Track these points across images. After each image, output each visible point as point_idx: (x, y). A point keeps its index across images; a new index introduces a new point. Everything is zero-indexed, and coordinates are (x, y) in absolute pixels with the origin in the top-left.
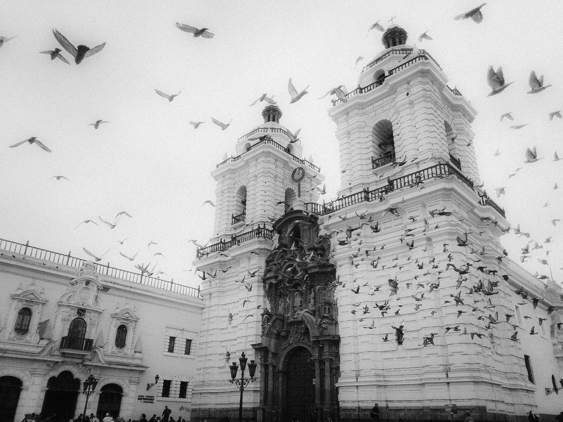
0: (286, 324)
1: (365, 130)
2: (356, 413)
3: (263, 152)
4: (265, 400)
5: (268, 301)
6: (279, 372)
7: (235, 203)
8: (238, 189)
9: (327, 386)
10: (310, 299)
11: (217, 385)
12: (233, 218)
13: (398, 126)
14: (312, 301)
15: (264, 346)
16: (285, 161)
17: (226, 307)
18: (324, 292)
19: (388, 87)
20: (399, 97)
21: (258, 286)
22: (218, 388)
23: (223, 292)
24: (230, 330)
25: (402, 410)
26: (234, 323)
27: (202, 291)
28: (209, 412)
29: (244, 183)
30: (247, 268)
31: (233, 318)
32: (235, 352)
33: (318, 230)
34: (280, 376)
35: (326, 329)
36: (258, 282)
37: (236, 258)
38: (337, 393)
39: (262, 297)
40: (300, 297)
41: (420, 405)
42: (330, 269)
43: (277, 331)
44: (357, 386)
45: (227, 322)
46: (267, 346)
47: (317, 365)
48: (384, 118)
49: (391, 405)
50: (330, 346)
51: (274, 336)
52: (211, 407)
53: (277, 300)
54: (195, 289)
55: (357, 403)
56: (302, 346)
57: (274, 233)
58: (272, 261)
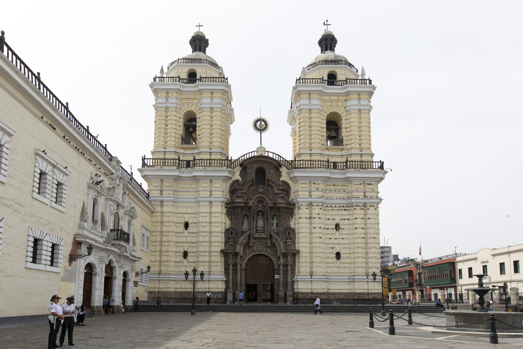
0: (252, 237)
1: (322, 112)
2: (311, 295)
3: (222, 90)
5: (227, 218)
7: (182, 124)
8: (185, 112)
9: (289, 280)
10: (272, 224)
11: (173, 275)
12: (182, 138)
13: (346, 122)
14: (275, 225)
17: (180, 215)
18: (284, 220)
19: (346, 91)
20: (352, 101)
21: (222, 206)
23: (176, 202)
25: (337, 294)
26: (191, 229)
27: (152, 197)
29: (193, 108)
30: (208, 189)
31: (189, 225)
32: (194, 252)
33: (280, 175)
35: (290, 245)
36: (222, 202)
37: (197, 177)
41: (348, 291)
42: (291, 207)
43: (246, 243)
45: (184, 229)
47: (281, 267)
48: (337, 111)
49: (330, 291)
51: (243, 245)
53: (241, 219)
55: (311, 290)
56: (264, 254)
57: (233, 166)
58: (242, 189)
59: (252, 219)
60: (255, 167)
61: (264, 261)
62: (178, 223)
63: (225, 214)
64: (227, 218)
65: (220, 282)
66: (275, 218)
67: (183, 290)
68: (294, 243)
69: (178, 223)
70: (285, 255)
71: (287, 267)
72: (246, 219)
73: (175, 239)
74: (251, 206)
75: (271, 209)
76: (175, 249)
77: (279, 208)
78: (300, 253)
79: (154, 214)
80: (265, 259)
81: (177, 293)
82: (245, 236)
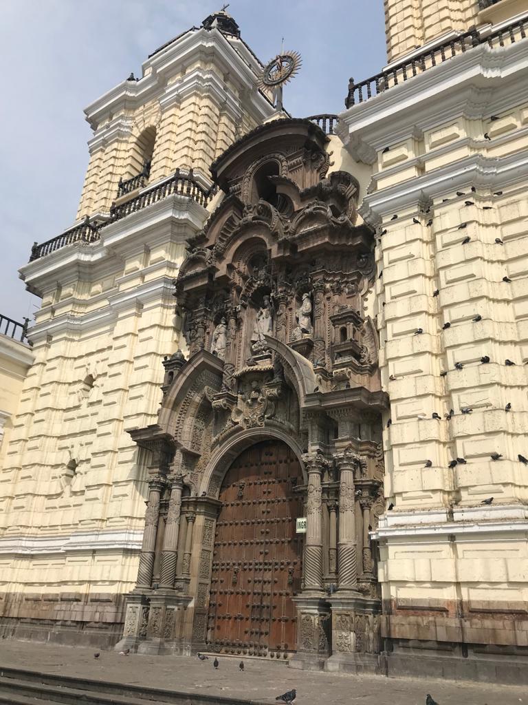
4: (150, 577)
5: (183, 341)
6: (197, 503)
11: (34, 538)
12: (121, 185)
15: (163, 432)
16: (242, 85)
22: (36, 544)
24: (85, 410)
28: (7, 601)
34: (200, 513)
38: (376, 556)
39: (171, 332)
40: (270, 318)
43: (204, 398)
44: (452, 537)
46: (172, 433)
50: (357, 427)
51: (192, 410)
52: (13, 591)
54: (16, 324)
55: (453, 589)
56: (268, 433)
59: (232, 321)
60: (251, 170)
61: (283, 465)
62: (75, 383)
63: (176, 329)
64: (185, 339)
65: (120, 558)
66: (304, 297)
67: (43, 590)
68: (374, 369)
69: (75, 383)
70: (327, 423)
71: (337, 477)
72: (221, 327)
73: (57, 431)
74: (225, 278)
75: (288, 271)
76: (53, 458)
77: (312, 258)
78: (393, 406)
79: (31, 371)
80: (284, 458)
81: (27, 600)
82: (188, 374)
